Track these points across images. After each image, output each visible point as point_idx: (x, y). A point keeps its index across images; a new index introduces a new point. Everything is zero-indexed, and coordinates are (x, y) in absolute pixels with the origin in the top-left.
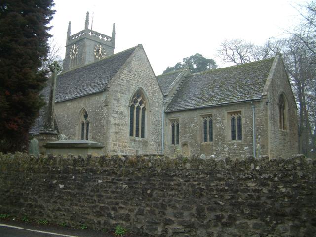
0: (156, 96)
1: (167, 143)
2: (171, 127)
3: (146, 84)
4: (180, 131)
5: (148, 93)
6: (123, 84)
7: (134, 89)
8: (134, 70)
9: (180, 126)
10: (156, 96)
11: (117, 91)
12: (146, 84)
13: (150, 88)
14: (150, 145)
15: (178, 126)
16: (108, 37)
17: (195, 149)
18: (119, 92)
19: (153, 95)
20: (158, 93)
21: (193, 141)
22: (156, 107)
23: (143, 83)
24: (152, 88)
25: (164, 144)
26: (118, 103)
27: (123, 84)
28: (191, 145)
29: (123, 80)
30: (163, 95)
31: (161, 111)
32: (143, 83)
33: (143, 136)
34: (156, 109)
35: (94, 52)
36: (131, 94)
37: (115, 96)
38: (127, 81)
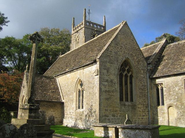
0: (141, 64)
1: (153, 105)
2: (155, 90)
3: (132, 55)
4: (165, 93)
5: (133, 63)
6: (112, 55)
7: (121, 59)
8: (120, 43)
9: (164, 89)
10: (141, 64)
11: (106, 62)
12: (132, 55)
13: (135, 58)
14: (139, 108)
15: (162, 90)
16: (101, 26)
17: (181, 111)
18: (109, 62)
19: (139, 63)
20: (142, 61)
21: (179, 104)
22: (141, 74)
23: (129, 54)
24: (137, 58)
25: (150, 105)
26: (108, 72)
27: (112, 55)
28: (177, 107)
29: (111, 52)
30: (147, 63)
31: (146, 77)
32: (129, 54)
33: (132, 100)
34: (142, 76)
35: (91, 36)
36: (119, 64)
37: (105, 66)
38: (115, 52)
